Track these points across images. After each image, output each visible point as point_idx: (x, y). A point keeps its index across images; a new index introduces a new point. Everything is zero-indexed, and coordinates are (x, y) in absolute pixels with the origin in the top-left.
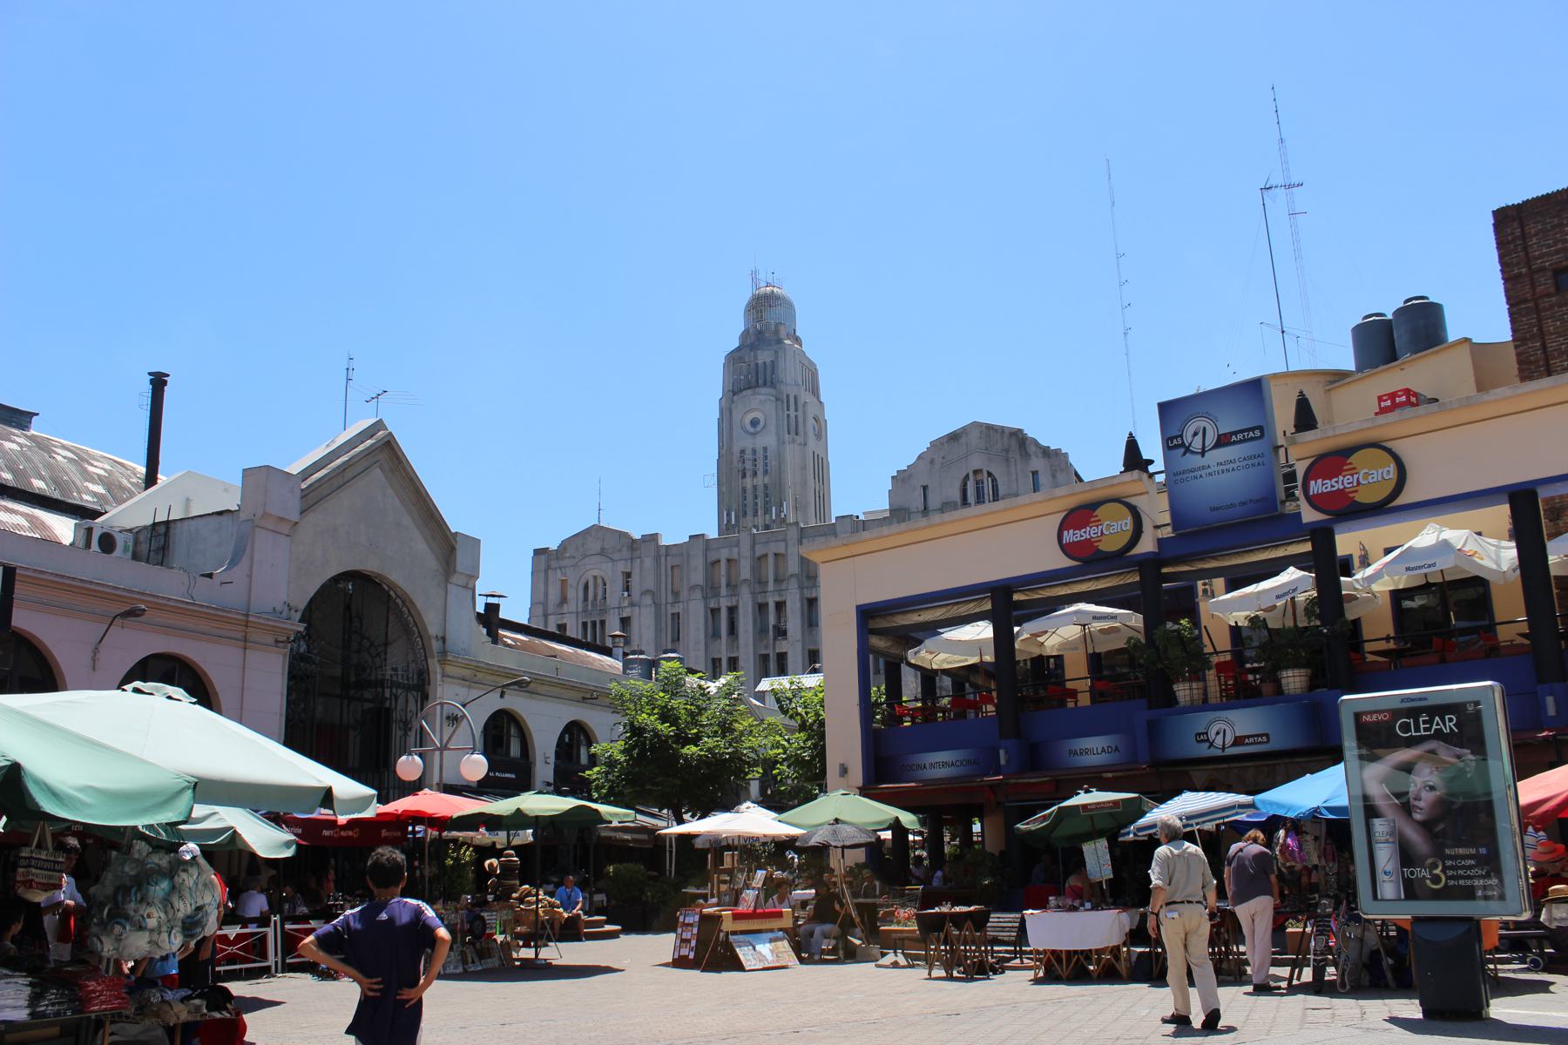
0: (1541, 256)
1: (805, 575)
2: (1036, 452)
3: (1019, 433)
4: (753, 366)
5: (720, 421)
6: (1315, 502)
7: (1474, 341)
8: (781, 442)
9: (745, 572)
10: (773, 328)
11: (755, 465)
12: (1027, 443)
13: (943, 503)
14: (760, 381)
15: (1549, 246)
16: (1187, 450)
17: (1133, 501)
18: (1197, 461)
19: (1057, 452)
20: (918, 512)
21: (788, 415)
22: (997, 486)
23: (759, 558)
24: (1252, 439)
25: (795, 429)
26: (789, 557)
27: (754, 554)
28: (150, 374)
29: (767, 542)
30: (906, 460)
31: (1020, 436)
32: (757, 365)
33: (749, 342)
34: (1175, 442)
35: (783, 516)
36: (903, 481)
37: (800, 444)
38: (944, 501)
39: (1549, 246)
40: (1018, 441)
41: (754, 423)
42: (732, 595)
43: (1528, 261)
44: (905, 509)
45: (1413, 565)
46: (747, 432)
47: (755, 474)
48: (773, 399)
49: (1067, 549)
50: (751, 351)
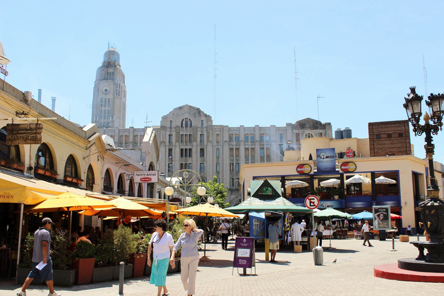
0: (375, 132)
1: (134, 142)
2: (203, 115)
5: (95, 88)
7: (357, 138)
8: (114, 98)
10: (113, 61)
11: (105, 104)
12: (201, 112)
13: (176, 126)
14: (109, 78)
15: (376, 131)
16: (321, 158)
17: (310, 165)
18: (322, 160)
19: (209, 116)
20: (169, 128)
21: (117, 89)
22: (191, 123)
23: (121, 136)
24: (332, 158)
26: (130, 136)
27: (119, 134)
28: (52, 97)
29: (123, 132)
30: (166, 113)
31: (199, 110)
32: (108, 72)
33: (106, 65)
36: (165, 119)
37: (120, 99)
38: (176, 126)
39: (376, 131)
40: (199, 111)
41: (106, 90)
43: (373, 133)
44: (165, 127)
46: (104, 93)
47: (105, 106)
48: (113, 84)
49: (298, 172)
50: (106, 68)
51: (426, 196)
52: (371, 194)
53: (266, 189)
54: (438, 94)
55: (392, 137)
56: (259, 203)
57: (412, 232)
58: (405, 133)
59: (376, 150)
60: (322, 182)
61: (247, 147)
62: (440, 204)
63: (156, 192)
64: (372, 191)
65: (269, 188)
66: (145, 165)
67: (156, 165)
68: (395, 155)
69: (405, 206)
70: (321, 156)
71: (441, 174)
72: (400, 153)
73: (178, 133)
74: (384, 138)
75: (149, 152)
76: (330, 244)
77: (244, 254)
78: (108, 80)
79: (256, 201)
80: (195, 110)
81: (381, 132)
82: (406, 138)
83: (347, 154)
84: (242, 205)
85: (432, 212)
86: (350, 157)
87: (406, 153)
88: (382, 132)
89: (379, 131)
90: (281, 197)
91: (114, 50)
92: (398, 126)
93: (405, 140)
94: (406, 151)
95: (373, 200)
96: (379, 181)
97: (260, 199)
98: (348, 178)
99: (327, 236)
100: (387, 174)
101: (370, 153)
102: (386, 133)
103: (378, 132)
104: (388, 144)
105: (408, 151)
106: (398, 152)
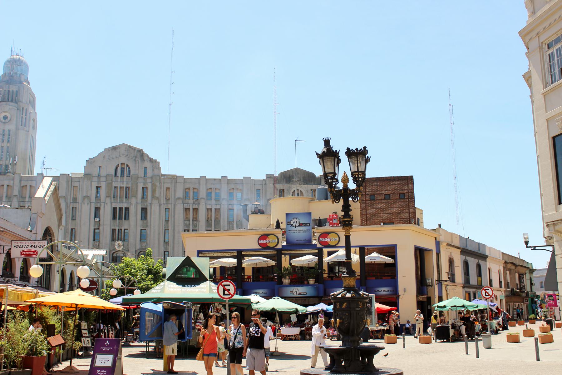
2: (147, 160)
3: (141, 151)
4: (7, 91)
6: (320, 243)
8: (17, 129)
9: (16, 192)
10: (18, 75)
11: (4, 137)
12: (144, 155)
13: (108, 175)
14: (10, 99)
15: (370, 190)
16: (292, 225)
17: (277, 235)
18: (294, 228)
19: (156, 161)
20: (96, 177)
21: (22, 117)
22: (130, 170)
23: (23, 187)
25: (24, 124)
31: (142, 152)
32: (9, 91)
34: (289, 223)
35: (15, 162)
36: (91, 163)
37: (26, 131)
39: (370, 190)
40: (141, 154)
42: (8, 201)
45: (339, 259)
48: (16, 108)
49: (260, 244)
50: (7, 84)
51: (436, 280)
52: (359, 277)
53: (187, 270)
54: (355, 149)
55: (391, 198)
56: (175, 290)
57: (412, 330)
58: (408, 194)
59: (369, 216)
60: (294, 260)
61: (209, 207)
62: (353, 295)
63: (56, 271)
64: (360, 273)
65: (191, 268)
66: (36, 231)
67: (57, 231)
68: (394, 224)
69: (404, 294)
70: (292, 223)
71: (460, 250)
72: (401, 220)
73: (109, 185)
74: (380, 200)
75: (43, 213)
76: (276, 347)
77: (104, 361)
78: (8, 103)
79: (172, 286)
80: (136, 151)
81: (376, 191)
82: (409, 200)
83: (330, 221)
84: (152, 291)
85: (344, 306)
86: (334, 225)
87: (408, 221)
88: (378, 191)
89: (373, 189)
90: (208, 281)
91: (20, 58)
92: (399, 184)
93: (408, 202)
94: (409, 218)
95: (361, 286)
96: (370, 260)
97: (178, 284)
98: (330, 254)
99: (292, 335)
100: (383, 250)
101: (361, 220)
102: (383, 194)
103: (373, 191)
104: (385, 208)
105: (411, 218)
106: (398, 219)
